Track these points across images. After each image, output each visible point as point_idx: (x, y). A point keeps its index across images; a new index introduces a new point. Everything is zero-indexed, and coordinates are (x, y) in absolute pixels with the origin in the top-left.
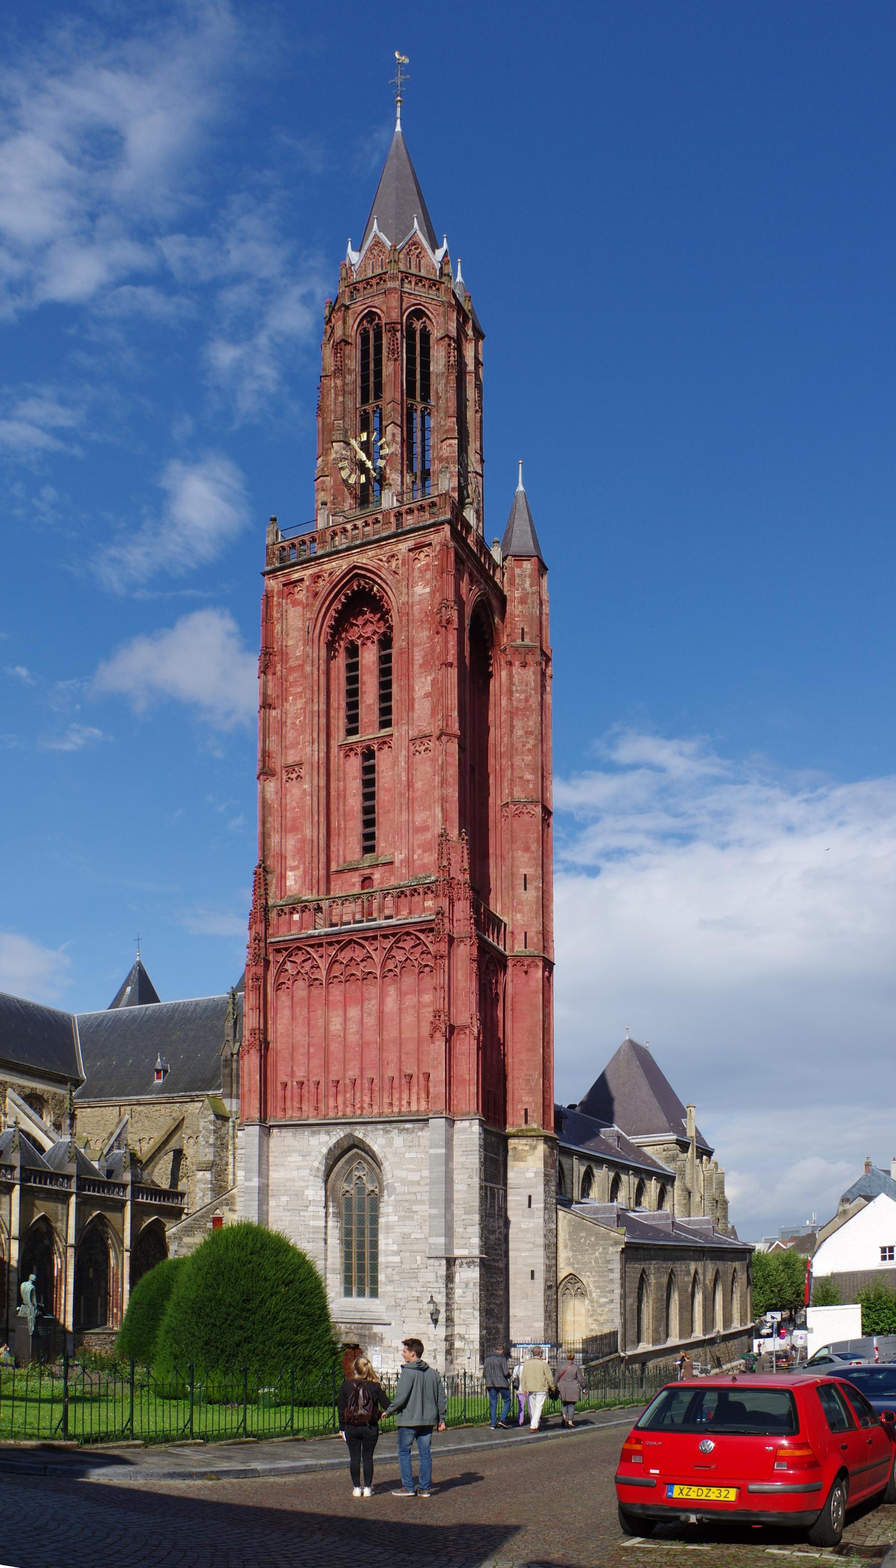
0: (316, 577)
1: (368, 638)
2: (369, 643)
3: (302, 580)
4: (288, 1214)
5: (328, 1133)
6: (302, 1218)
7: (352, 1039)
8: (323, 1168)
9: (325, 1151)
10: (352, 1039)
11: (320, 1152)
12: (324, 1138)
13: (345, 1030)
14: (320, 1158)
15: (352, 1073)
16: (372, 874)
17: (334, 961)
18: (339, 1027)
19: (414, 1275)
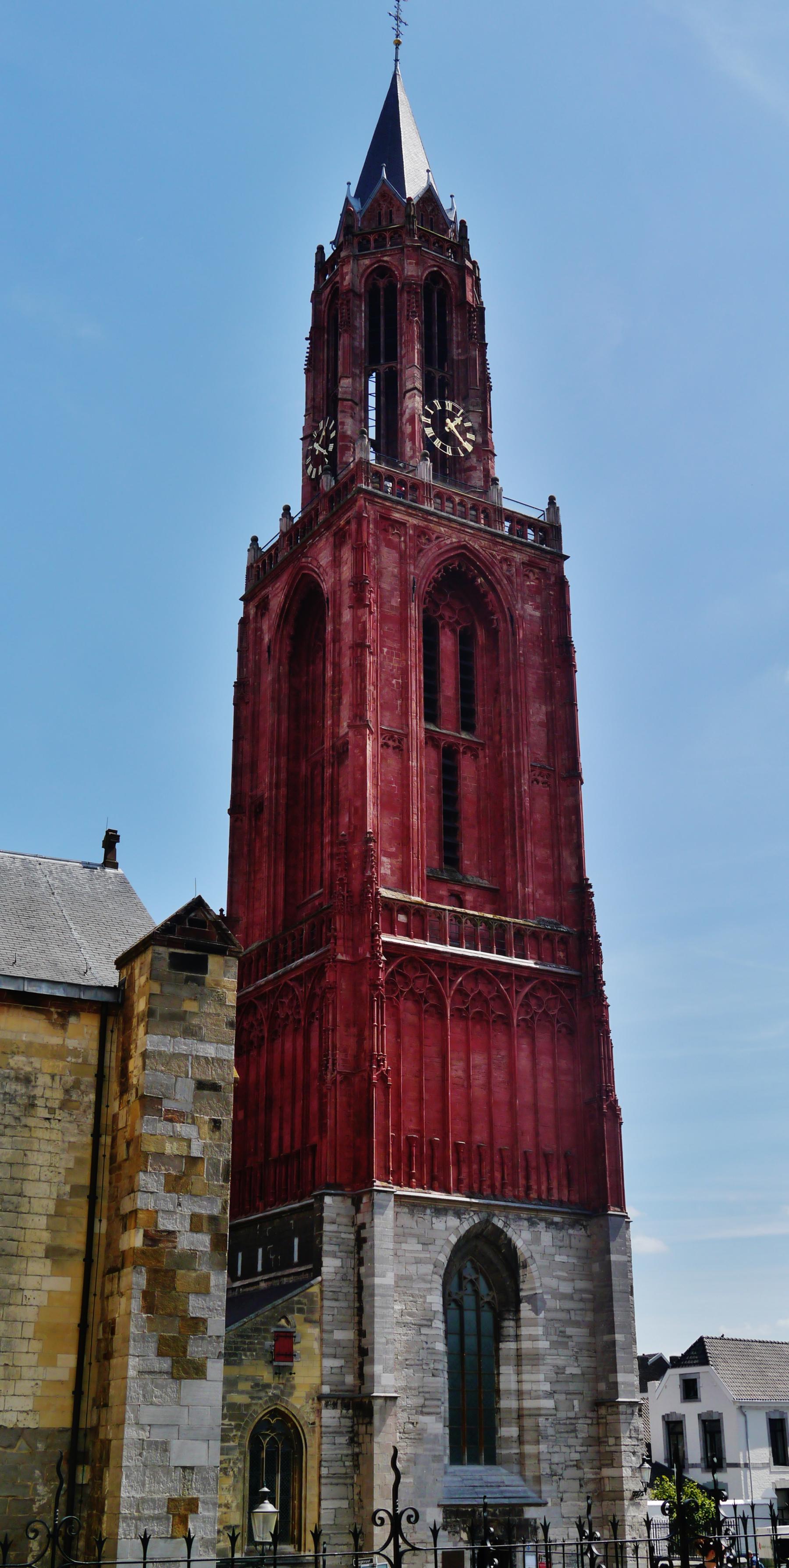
0: (421, 532)
1: (449, 624)
2: (447, 630)
3: (403, 524)
4: (402, 1330)
5: (458, 1215)
6: (423, 1338)
7: (478, 1092)
8: (446, 1263)
9: (454, 1239)
10: (478, 1092)
11: (448, 1241)
12: (452, 1221)
13: (468, 1077)
14: (448, 1251)
15: (480, 1136)
16: (464, 893)
17: (460, 991)
18: (460, 1073)
19: (572, 1427)
